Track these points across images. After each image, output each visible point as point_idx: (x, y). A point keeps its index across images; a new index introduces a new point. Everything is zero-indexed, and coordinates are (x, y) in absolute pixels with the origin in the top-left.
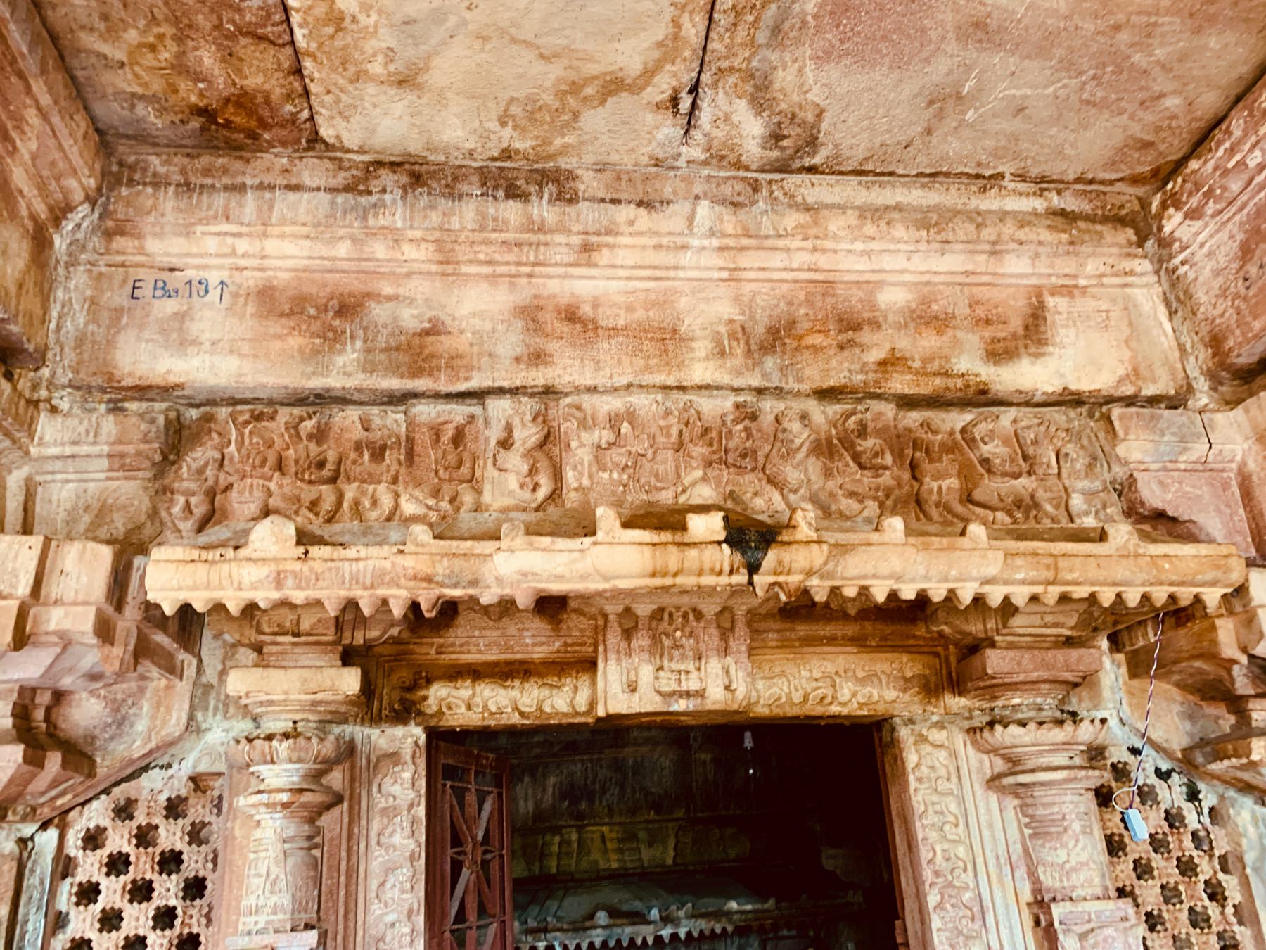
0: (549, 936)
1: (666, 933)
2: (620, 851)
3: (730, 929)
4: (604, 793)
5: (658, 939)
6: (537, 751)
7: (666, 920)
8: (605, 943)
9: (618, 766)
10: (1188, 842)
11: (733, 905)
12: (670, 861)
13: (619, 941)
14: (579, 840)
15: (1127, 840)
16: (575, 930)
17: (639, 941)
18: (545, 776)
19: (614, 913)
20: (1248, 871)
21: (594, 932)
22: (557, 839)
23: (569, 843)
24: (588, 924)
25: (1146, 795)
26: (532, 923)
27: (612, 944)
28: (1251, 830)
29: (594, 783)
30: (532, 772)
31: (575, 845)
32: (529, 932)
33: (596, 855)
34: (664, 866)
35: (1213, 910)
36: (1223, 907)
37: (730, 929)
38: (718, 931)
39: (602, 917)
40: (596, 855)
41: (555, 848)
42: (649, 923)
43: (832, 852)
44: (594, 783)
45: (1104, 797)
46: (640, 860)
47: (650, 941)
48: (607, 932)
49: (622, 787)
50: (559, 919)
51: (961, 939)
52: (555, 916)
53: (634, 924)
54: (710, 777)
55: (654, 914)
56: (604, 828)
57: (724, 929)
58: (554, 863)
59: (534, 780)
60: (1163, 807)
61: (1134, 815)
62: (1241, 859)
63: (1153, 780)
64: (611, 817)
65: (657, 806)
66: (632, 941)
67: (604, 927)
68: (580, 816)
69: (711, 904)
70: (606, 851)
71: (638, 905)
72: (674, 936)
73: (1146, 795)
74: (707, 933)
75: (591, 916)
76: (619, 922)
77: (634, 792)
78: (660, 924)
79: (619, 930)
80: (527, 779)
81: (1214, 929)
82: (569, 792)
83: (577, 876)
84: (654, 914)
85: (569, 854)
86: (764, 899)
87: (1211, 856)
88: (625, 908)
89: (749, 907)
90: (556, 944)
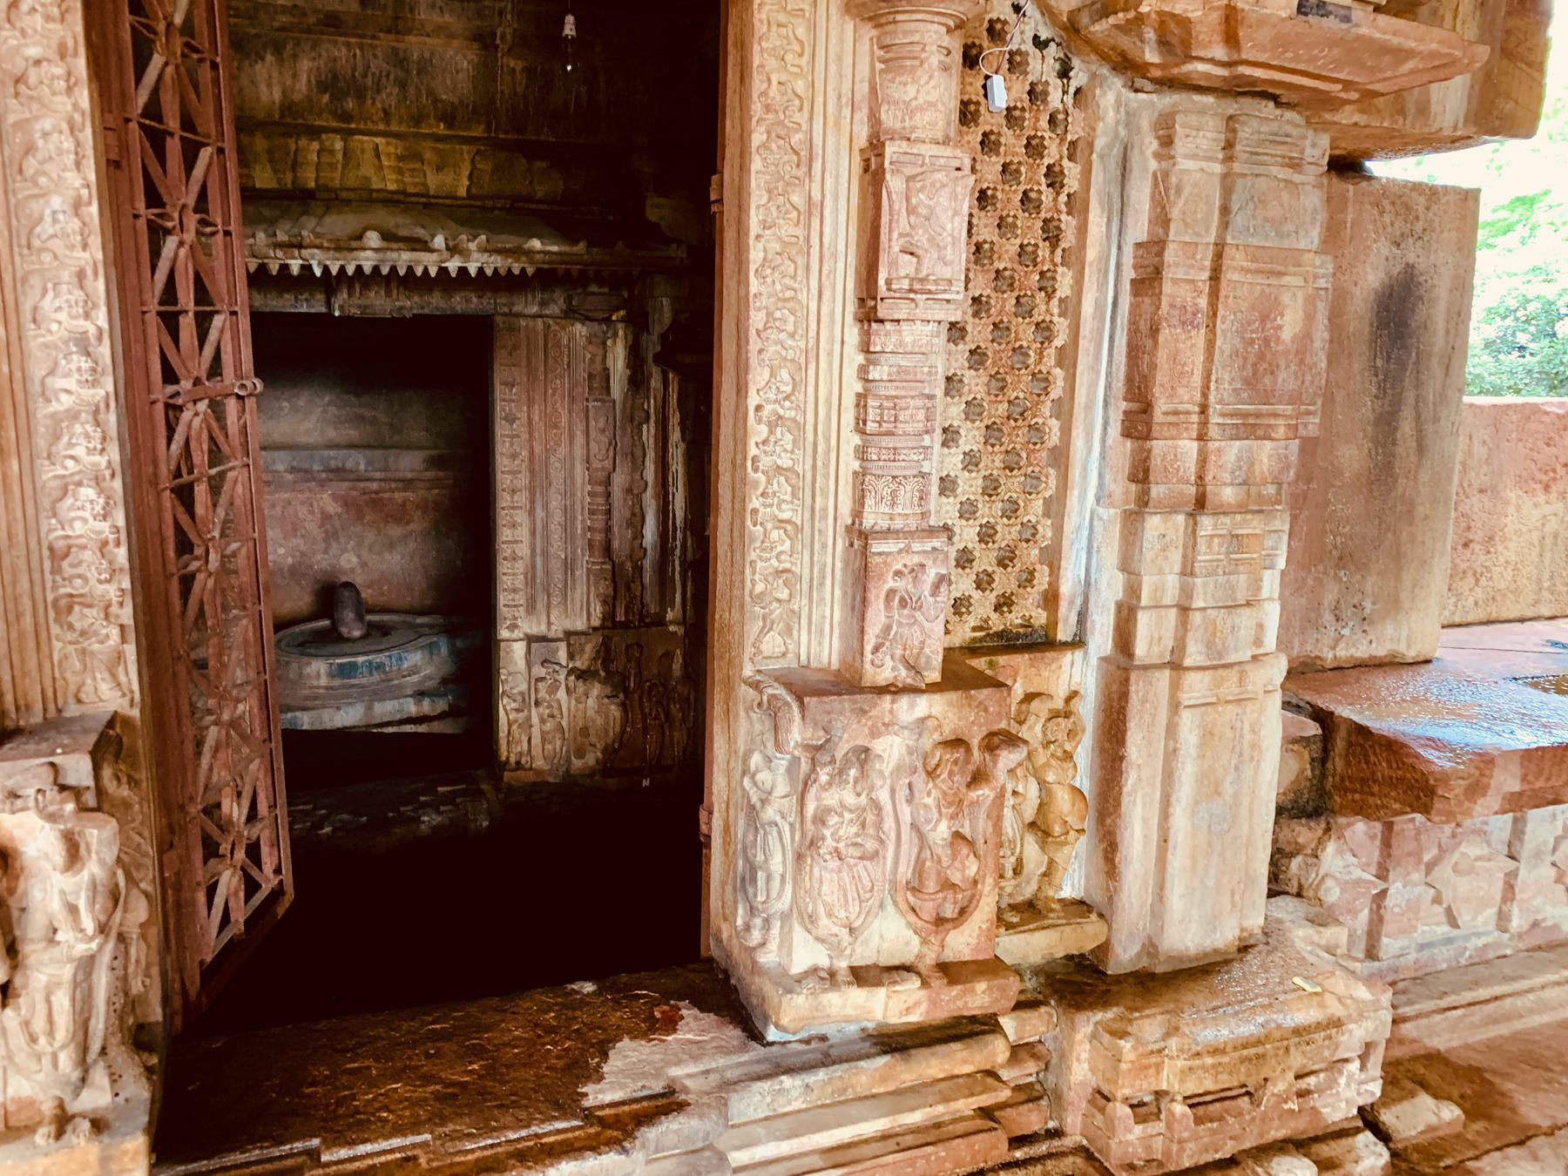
0: (305, 252)
1: (453, 265)
2: (400, 171)
3: (530, 271)
4: (378, 92)
5: (443, 271)
6: (284, 19)
7: (453, 250)
8: (376, 269)
9: (399, 60)
10: (1044, 123)
11: (536, 244)
12: (462, 192)
13: (393, 269)
14: (345, 149)
15: (982, 109)
16: (338, 249)
17: (419, 271)
18: (295, 57)
19: (387, 236)
20: (1094, 156)
22: (315, 146)
23: (332, 152)
24: (354, 244)
25: (1016, 63)
26: (282, 237)
27: (385, 270)
28: (1111, 113)
29: (365, 76)
30: (278, 49)
33: (367, 169)
34: (456, 198)
35: (1047, 196)
36: (1058, 194)
37: (530, 271)
38: (516, 272)
39: (373, 238)
40: (367, 169)
42: (432, 251)
43: (663, 201)
45: (971, 59)
46: (425, 185)
47: (433, 272)
48: (381, 255)
49: (403, 85)
50: (317, 235)
51: (781, 184)
52: (313, 231)
53: (413, 250)
54: (520, 90)
55: (439, 241)
56: (378, 140)
57: (523, 270)
58: (313, 176)
59: (280, 61)
60: (1030, 78)
61: (998, 82)
62: (1091, 145)
63: (1028, 47)
64: (388, 124)
65: (449, 118)
66: (410, 269)
68: (346, 117)
69: (510, 241)
70: (381, 167)
71: (420, 232)
72: (463, 271)
73: (1016, 63)
74: (502, 272)
75: (360, 237)
76: (395, 246)
77: (418, 97)
78: (446, 254)
79: (394, 255)
80: (269, 58)
81: (1043, 215)
82: (331, 84)
83: (344, 195)
84: (439, 241)
85: (332, 166)
86: (576, 242)
87: (1062, 140)
88: (403, 233)
89: (555, 248)
90: (314, 264)
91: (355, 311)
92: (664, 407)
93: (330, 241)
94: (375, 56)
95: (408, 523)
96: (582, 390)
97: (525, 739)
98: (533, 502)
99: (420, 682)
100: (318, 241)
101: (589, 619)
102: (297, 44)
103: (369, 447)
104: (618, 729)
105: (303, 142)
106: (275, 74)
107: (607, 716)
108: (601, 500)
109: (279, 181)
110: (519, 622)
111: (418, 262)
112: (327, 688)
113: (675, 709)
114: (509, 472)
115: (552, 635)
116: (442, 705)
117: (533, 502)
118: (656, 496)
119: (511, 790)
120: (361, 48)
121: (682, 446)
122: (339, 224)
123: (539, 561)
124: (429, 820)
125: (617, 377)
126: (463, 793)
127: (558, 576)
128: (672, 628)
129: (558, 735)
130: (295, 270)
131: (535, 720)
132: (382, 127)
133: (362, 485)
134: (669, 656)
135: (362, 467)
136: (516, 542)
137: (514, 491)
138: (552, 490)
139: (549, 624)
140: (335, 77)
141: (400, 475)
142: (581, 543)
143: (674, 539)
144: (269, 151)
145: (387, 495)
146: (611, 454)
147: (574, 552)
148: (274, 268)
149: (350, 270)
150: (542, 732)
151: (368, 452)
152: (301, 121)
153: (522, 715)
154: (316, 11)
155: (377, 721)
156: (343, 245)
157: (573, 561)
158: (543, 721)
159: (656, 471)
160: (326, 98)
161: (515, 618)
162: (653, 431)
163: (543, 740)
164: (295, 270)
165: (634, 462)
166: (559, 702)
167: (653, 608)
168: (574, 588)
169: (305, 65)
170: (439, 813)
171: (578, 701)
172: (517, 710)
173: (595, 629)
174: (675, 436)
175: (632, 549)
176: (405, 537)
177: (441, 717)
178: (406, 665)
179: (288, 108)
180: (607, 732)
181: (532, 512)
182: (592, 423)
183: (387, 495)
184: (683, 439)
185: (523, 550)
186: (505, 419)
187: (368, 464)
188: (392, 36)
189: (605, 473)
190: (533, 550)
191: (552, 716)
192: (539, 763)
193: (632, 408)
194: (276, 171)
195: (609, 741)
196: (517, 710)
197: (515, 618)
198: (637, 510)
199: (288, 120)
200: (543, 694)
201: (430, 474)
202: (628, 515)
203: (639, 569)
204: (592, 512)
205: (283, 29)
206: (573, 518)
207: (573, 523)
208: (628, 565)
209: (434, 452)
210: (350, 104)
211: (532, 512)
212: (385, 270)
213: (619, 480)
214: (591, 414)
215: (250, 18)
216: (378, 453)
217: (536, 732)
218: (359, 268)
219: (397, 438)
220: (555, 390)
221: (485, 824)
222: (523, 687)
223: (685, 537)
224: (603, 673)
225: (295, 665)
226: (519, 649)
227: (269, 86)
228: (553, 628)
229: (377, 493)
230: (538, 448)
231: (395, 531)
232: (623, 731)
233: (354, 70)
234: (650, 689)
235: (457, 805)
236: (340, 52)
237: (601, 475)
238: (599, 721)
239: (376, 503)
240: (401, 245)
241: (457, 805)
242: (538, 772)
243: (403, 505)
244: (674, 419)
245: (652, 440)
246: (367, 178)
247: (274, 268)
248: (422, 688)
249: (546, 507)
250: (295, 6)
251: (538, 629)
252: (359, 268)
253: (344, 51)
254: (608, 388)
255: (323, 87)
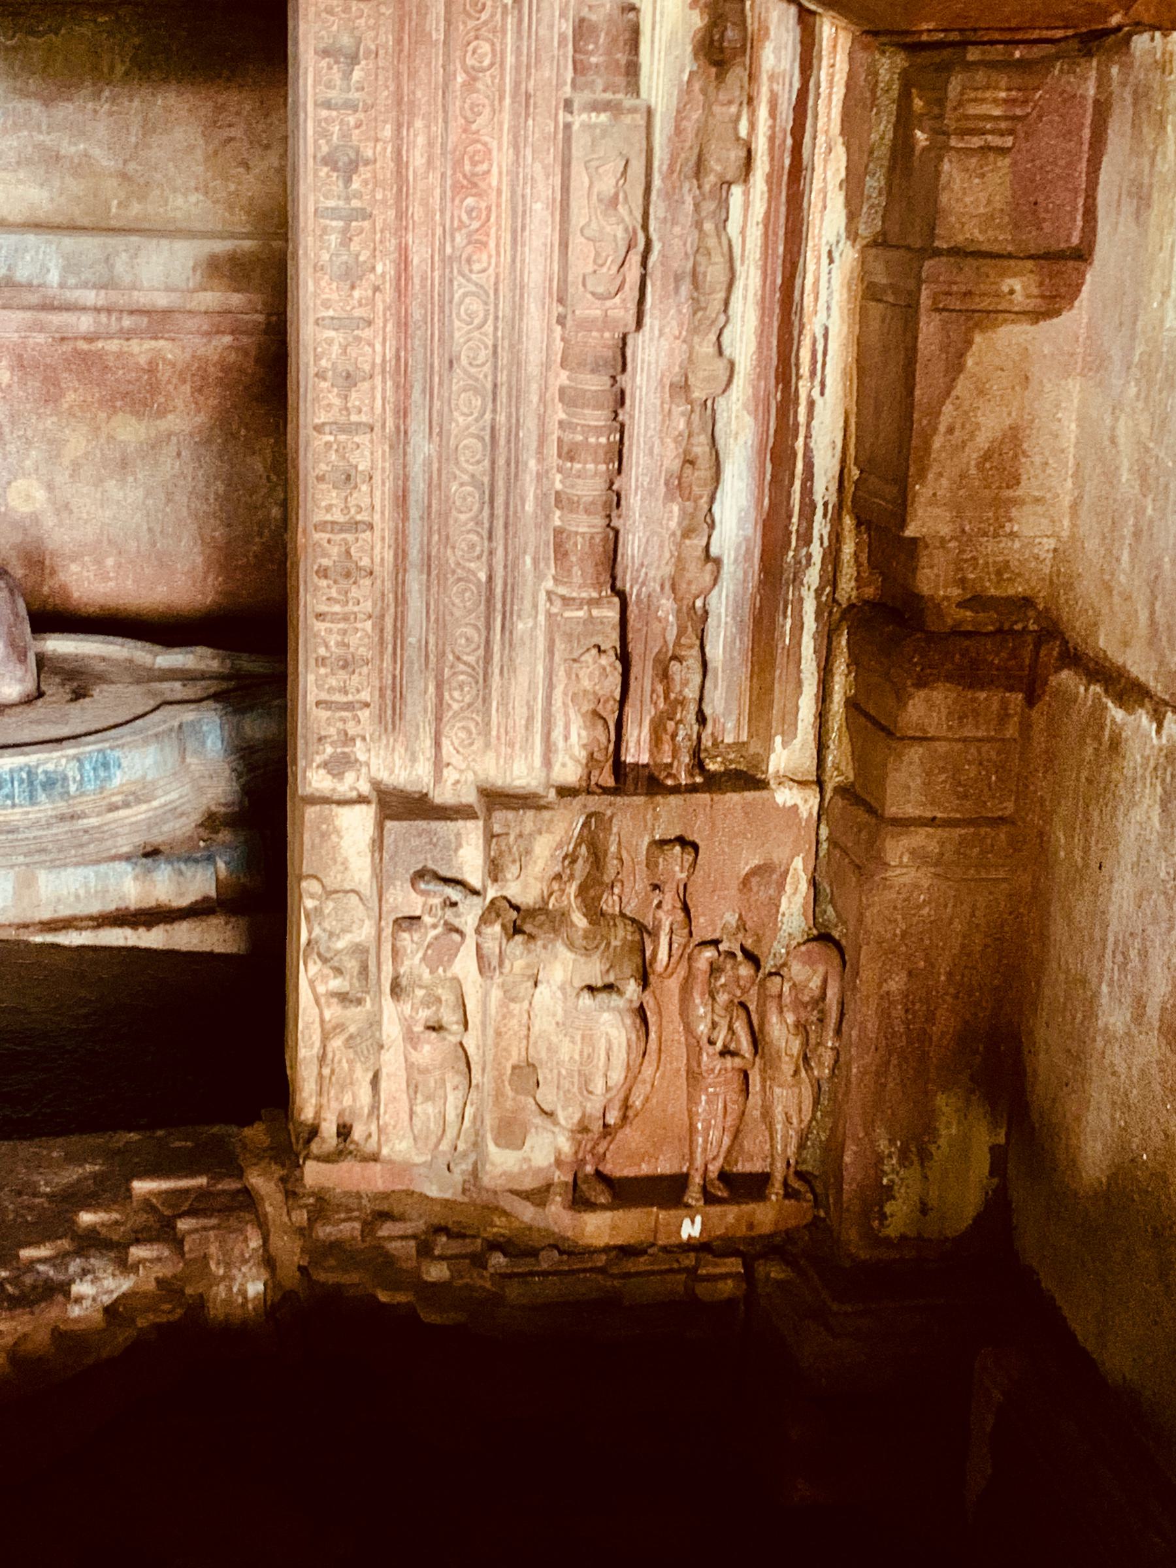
92: (798, 131)
95: (162, 413)
96: (554, 72)
97: (363, 1078)
98: (402, 413)
99: (151, 824)
101: (548, 763)
103: (73, 228)
104: (617, 1076)
107: (588, 1039)
108: (598, 417)
110: (359, 751)
113: (780, 1031)
114: (337, 323)
115: (443, 796)
116: (200, 883)
117: (402, 413)
118: (759, 405)
119: (322, 1206)
121: (848, 255)
123: (415, 582)
124: (95, 1290)
125: (663, 34)
126: (199, 1204)
127: (466, 634)
128: (785, 796)
129: (453, 1079)
131: (391, 1030)
133: (56, 319)
134: (768, 874)
135: (54, 277)
136: (354, 526)
137: (349, 380)
138: (458, 380)
139: (439, 765)
141: (141, 299)
142: (533, 540)
143: (806, 538)
145: (113, 346)
146: (633, 273)
147: (512, 567)
150: (410, 1066)
151: (69, 242)
153: (354, 1016)
155: (46, 915)
157: (511, 588)
158: (411, 1039)
159: (762, 334)
161: (348, 740)
162: (759, 208)
163: (413, 1088)
165: (697, 307)
166: (457, 983)
167: (728, 723)
168: (509, 667)
170: (124, 1266)
171: (510, 996)
172: (343, 998)
173: (565, 792)
174: (828, 219)
175: (680, 563)
176: (155, 445)
177: (197, 911)
178: (118, 779)
180: (586, 1087)
181: (400, 440)
182: (580, 178)
183: (113, 346)
184: (852, 234)
185: (376, 550)
186: (329, 161)
187: (70, 266)
189: (610, 337)
190: (401, 554)
191: (436, 1028)
192: (399, 1147)
193: (703, 132)
195: (594, 1106)
196: (343, 998)
197: (348, 740)
198: (700, 448)
200: (413, 964)
201: (211, 299)
202: (672, 462)
203: (697, 621)
204: (569, 453)
206: (515, 465)
207: (514, 478)
208: (666, 606)
209: (221, 247)
211: (400, 440)
213: (654, 355)
214: (578, 152)
216: (90, 245)
217: (392, 1062)
219: (136, 208)
220: (472, 78)
221: (255, 1288)
222: (364, 933)
223: (836, 537)
224: (580, 921)
226: (355, 827)
228: (450, 775)
229: (90, 339)
230: (419, 256)
231: (130, 431)
232: (633, 1075)
234: (714, 969)
235: (177, 1243)
237: (601, 342)
238: (568, 1051)
239: (87, 363)
241: (177, 1243)
242: (404, 1168)
243: (151, 369)
244: (829, 169)
245: (755, 234)
248: (156, 838)
249: (437, 429)
251: (409, 772)
254: (632, 70)
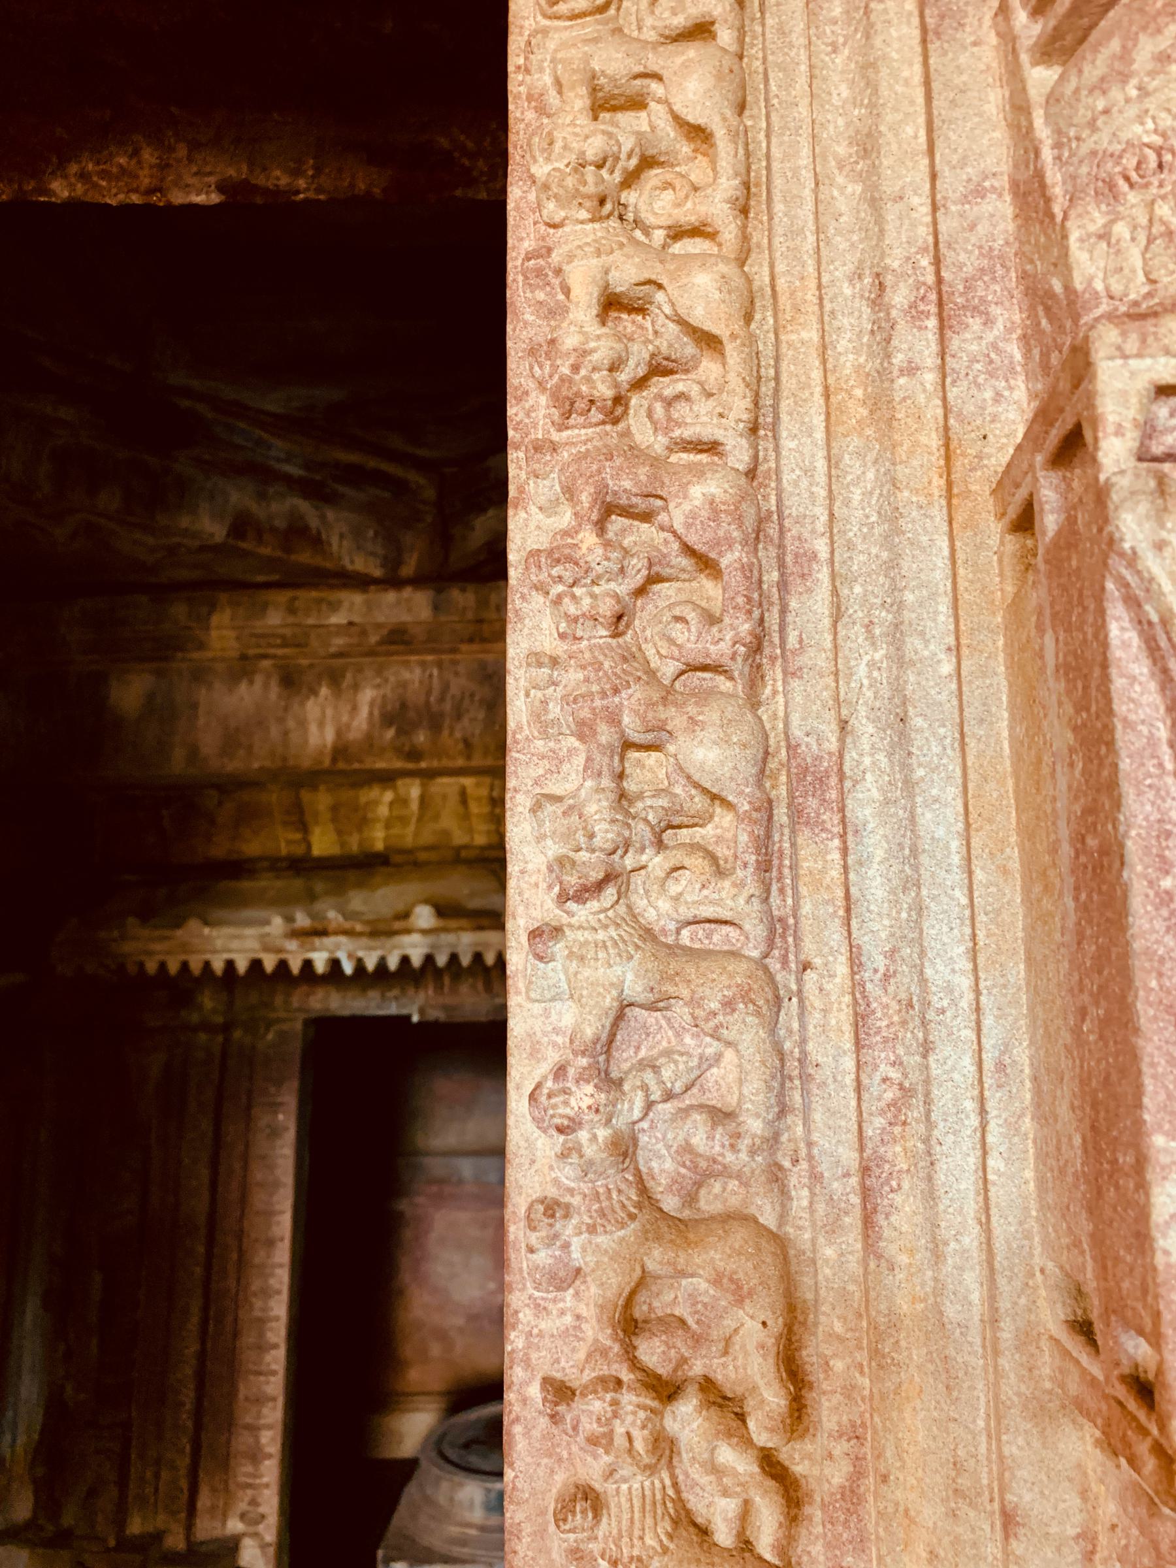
0: (329, 941)
4: (459, 717)
6: (339, 642)
8: (429, 959)
13: (454, 958)
14: (423, 801)
18: (356, 687)
19: (443, 910)
21: (406, 939)
22: (388, 796)
24: (397, 925)
26: (302, 920)
27: (441, 960)
30: (335, 679)
31: (414, 806)
32: (296, 934)
33: (448, 821)
41: (383, 811)
44: (442, 699)
53: (481, 928)
56: (468, 782)
64: (469, 758)
67: (424, 932)
68: (414, 755)
70: (466, 816)
75: (406, 915)
76: (453, 923)
80: (324, 691)
82: (397, 716)
83: (423, 856)
91: (435, 1014)
93: (368, 922)
94: (456, 674)
100: (347, 925)
102: (360, 670)
105: (374, 793)
106: (329, 712)
109: (343, 845)
111: (487, 945)
112: (483, 1528)
120: (440, 665)
122: (381, 898)
130: (320, 967)
132: (460, 762)
140: (404, 706)
144: (334, 808)
148: (295, 967)
149: (393, 963)
152: (356, 766)
154: (379, 626)
156: (382, 926)
160: (390, 733)
164: (320, 967)
169: (367, 695)
179: (341, 751)
188: (475, 647)
194: (340, 833)
199: (341, 765)
205: (340, 655)
210: (421, 738)
212: (441, 960)
215: (298, 646)
218: (405, 960)
225: (445, 1485)
227: (321, 725)
233: (429, 693)
236: (412, 675)
240: (463, 922)
246: (446, 833)
247: (295, 967)
250: (351, 624)
252: (405, 960)
253: (418, 671)
255: (388, 719)
